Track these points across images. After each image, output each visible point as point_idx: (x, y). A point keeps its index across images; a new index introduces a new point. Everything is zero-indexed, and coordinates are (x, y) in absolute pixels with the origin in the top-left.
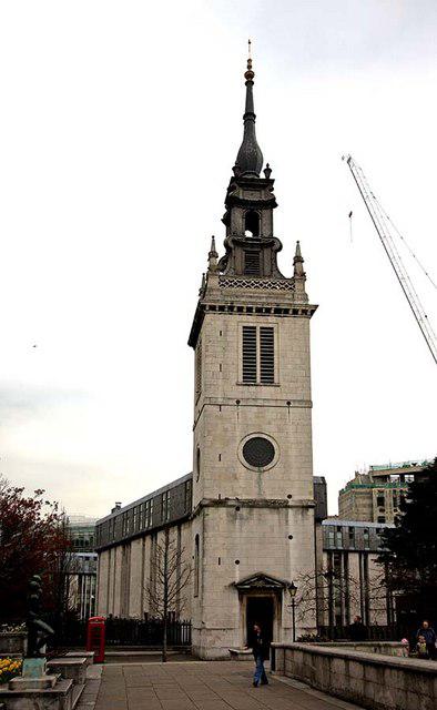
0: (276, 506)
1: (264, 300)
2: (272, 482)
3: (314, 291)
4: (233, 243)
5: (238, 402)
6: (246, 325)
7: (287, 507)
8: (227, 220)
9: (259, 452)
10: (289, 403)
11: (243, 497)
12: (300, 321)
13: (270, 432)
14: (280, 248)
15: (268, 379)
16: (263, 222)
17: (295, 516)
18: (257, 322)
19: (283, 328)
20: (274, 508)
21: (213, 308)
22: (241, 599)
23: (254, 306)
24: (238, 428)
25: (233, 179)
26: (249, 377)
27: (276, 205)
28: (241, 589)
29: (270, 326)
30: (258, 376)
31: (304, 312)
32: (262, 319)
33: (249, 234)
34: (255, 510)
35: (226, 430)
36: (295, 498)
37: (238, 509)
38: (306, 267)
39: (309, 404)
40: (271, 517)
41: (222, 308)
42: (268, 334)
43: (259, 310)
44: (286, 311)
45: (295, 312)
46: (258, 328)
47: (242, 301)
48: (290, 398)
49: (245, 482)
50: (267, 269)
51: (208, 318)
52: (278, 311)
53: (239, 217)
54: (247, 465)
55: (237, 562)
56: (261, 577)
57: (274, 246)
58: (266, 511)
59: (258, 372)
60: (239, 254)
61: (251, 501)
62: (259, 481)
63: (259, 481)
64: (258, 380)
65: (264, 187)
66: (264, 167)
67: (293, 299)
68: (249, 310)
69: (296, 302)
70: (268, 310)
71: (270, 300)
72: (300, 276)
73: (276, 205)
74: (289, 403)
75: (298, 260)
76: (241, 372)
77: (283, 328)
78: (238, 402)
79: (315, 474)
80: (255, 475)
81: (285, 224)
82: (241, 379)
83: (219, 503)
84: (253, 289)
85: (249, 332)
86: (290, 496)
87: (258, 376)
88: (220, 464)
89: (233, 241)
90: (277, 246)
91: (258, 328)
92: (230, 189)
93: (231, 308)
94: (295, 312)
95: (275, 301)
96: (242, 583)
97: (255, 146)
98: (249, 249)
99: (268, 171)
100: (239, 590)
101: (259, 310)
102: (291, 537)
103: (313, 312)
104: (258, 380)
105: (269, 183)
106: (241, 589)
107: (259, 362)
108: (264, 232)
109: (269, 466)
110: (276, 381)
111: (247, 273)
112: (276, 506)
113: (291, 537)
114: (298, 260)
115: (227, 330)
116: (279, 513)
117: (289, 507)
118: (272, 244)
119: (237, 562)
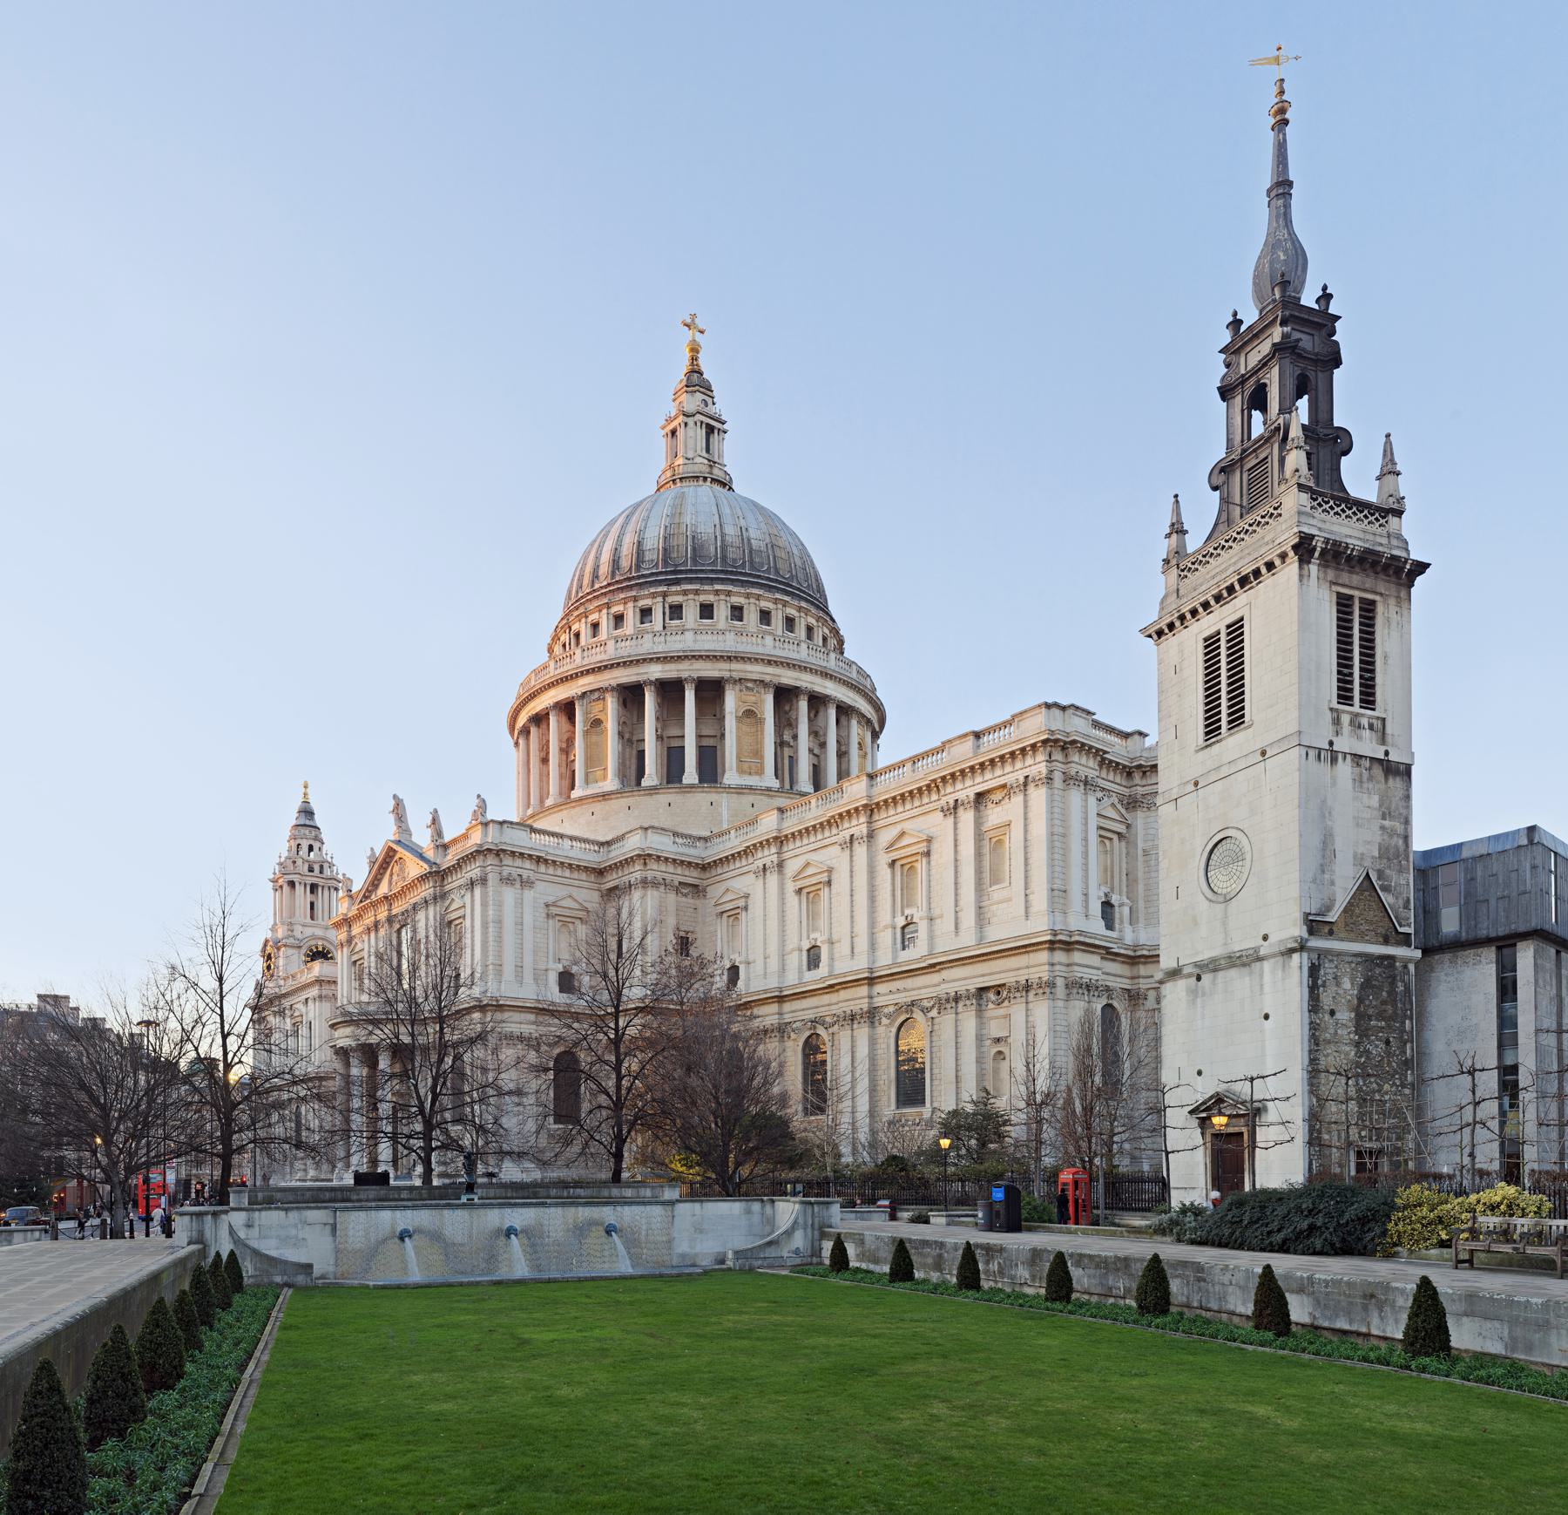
0: (1246, 960)
7: (1260, 959)
10: (1263, 753)
11: (1206, 955)
15: (1237, 719)
18: (1216, 621)
20: (1244, 965)
26: (1212, 730)
61: (1213, 960)
68: (1206, 605)
93: (1182, 618)
112: (1246, 960)
113: (1266, 1017)
116: (1251, 974)
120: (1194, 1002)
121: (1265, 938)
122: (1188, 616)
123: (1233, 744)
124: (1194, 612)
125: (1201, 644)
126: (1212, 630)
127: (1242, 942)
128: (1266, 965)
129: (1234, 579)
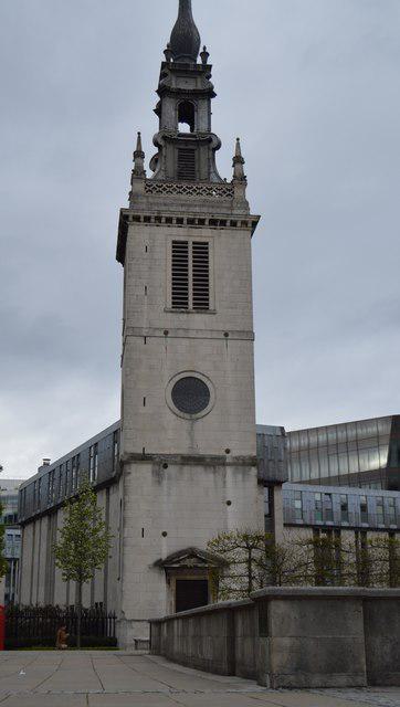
0: (214, 463)
1: (197, 209)
2: (210, 433)
3: (256, 198)
4: (165, 140)
5: (166, 333)
6: (177, 239)
7: (224, 464)
8: (158, 111)
9: (190, 395)
10: (226, 335)
12: (240, 234)
13: (204, 369)
14: (218, 146)
15: (202, 304)
16: (200, 115)
17: (234, 473)
19: (220, 245)
21: (137, 219)
22: (168, 582)
23: (185, 217)
24: (170, 363)
25: (164, 65)
26: (179, 302)
27: (214, 95)
28: (165, 566)
29: (203, 240)
30: (191, 302)
31: (245, 223)
32: (196, 232)
33: (184, 128)
34: (186, 469)
35: (151, 368)
36: (235, 453)
37: (165, 466)
38: (247, 169)
39: (248, 336)
40: (204, 477)
41: (147, 219)
42: (202, 250)
43: (191, 222)
44: (223, 223)
45: (234, 224)
46: (190, 246)
47: (176, 211)
48: (228, 327)
49: (170, 433)
50: (204, 170)
51: (137, 233)
52: (213, 222)
53: (171, 109)
54: (176, 410)
55: (164, 534)
56: (192, 553)
57: (210, 143)
58: (200, 469)
59: (191, 297)
60: (171, 153)
62: (191, 433)
63: (191, 433)
64: (191, 306)
65: (200, 73)
66: (201, 50)
67: (231, 208)
68: (180, 221)
69: (235, 212)
70: (202, 222)
71: (205, 210)
72: (240, 179)
73: (214, 95)
74: (226, 335)
75: (238, 160)
76: (170, 296)
77: (220, 245)
78: (166, 333)
79: (261, 420)
80: (186, 424)
81: (223, 119)
82: (170, 305)
83: (144, 458)
84: (184, 196)
85: (179, 248)
86: (228, 451)
87: (191, 302)
88: (143, 410)
89: (164, 138)
90: (215, 142)
91: (190, 246)
92: (163, 76)
93: (158, 219)
94: (234, 224)
95: (211, 210)
96: (170, 559)
97: (191, 25)
98: (182, 147)
99: (205, 55)
100: (166, 569)
101: (191, 222)
102: (229, 503)
103: (255, 224)
104: (191, 306)
105: (206, 70)
106: (165, 566)
107: (191, 283)
108: (202, 127)
109: (203, 413)
110: (211, 307)
111: (181, 176)
112: (214, 463)
113: (229, 503)
114: (238, 160)
115: (157, 243)
116: (214, 473)
117: (229, 464)
118: (210, 141)
119: (164, 534)
120: (159, 482)
121: (228, 451)
122: (163, 220)
123: (198, 320)
124: (169, 220)
125: (170, 245)
126: (182, 239)
127: (204, 449)
128: (229, 470)
129: (208, 217)
